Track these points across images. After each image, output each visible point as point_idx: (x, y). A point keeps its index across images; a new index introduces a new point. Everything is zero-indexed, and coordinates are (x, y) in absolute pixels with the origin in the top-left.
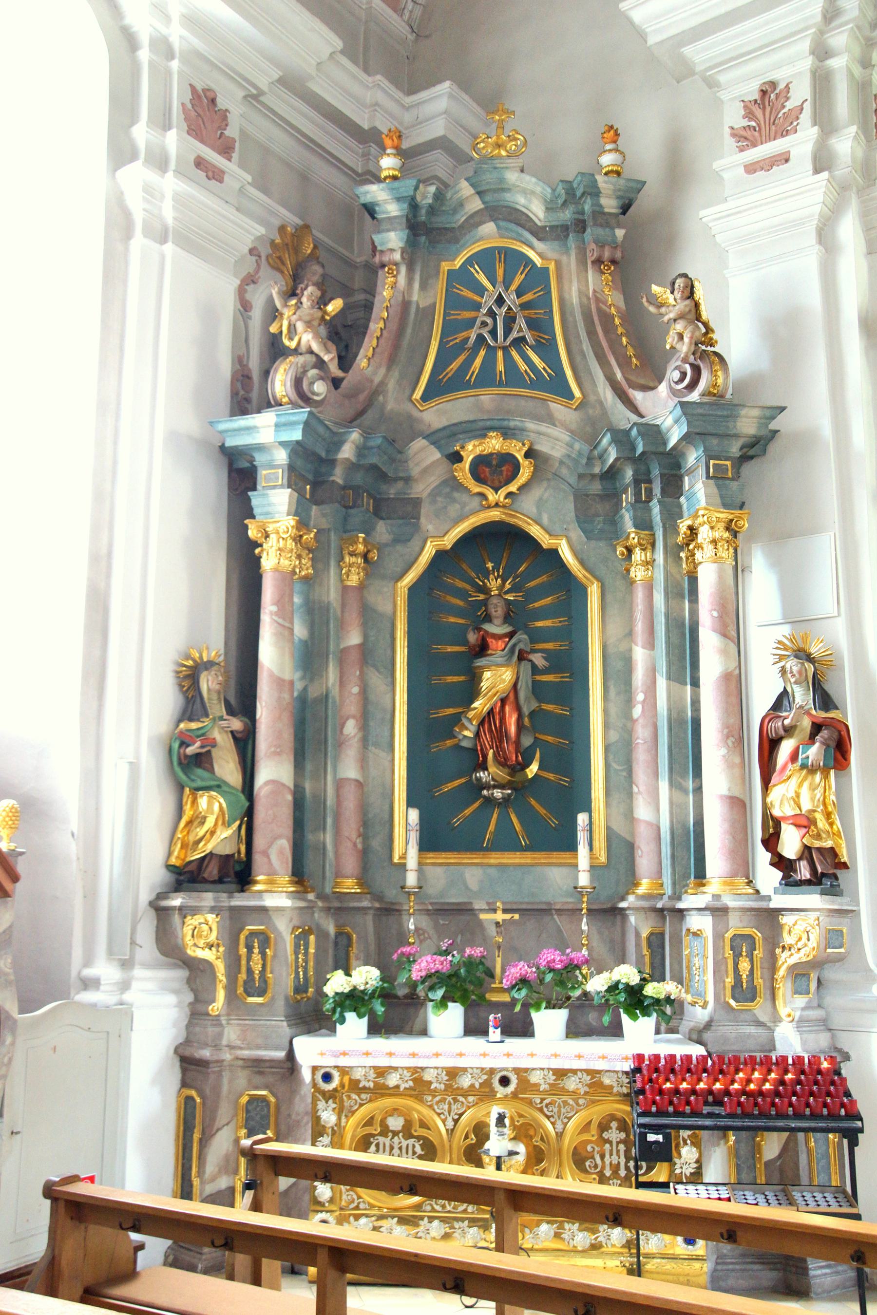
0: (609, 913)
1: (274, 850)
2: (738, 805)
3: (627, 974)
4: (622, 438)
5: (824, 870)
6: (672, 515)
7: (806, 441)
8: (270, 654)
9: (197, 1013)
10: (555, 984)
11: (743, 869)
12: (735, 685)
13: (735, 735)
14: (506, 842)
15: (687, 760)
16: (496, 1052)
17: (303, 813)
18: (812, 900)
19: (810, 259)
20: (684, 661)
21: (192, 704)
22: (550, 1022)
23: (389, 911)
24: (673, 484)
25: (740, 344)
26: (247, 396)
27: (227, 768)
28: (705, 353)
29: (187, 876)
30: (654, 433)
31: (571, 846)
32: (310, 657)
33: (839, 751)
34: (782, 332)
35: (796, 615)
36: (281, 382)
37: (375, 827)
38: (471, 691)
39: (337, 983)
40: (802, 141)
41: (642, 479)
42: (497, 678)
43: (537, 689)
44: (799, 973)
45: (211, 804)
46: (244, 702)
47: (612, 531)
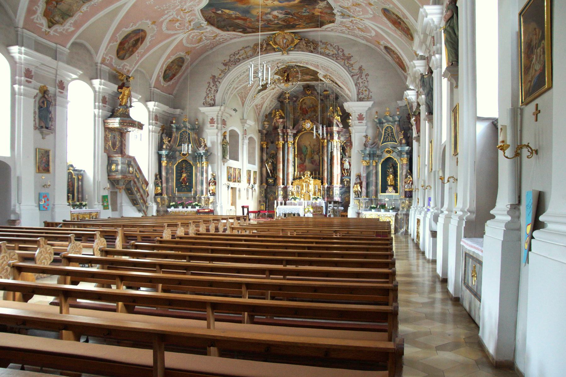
0: (195, 198)
1: (165, 192)
2: (207, 189)
3: (196, 203)
4: (197, 154)
5: (214, 194)
6: (202, 161)
7: (215, 154)
8: (164, 174)
9: (158, 207)
10: (190, 204)
11: (207, 194)
12: (207, 178)
13: (207, 182)
14: (184, 191)
15: (202, 184)
16: (185, 209)
17: (167, 188)
18: (212, 197)
19: (215, 137)
20: (202, 175)
21: (156, 179)
22: (190, 207)
23: (174, 198)
24: (202, 158)
25: (209, 145)
26: (160, 148)
27: (160, 185)
28: (205, 146)
29: (156, 195)
30: (200, 154)
31: (191, 191)
32: (167, 173)
33: (215, 184)
34: (213, 143)
35: (213, 171)
36: (164, 147)
37: (173, 189)
38: (181, 176)
39: (171, 204)
40: (215, 125)
41: (199, 157)
42: (184, 175)
43: (188, 176)
44: (211, 203)
45: (159, 188)
46: (161, 178)
47: (196, 162)
